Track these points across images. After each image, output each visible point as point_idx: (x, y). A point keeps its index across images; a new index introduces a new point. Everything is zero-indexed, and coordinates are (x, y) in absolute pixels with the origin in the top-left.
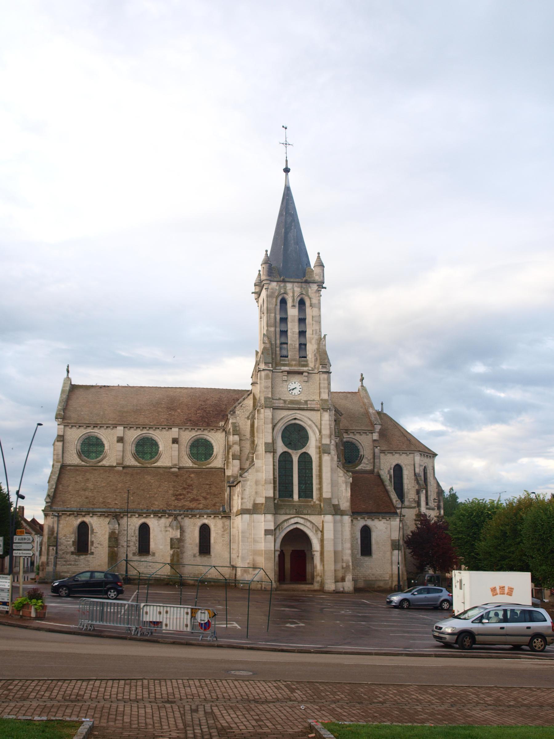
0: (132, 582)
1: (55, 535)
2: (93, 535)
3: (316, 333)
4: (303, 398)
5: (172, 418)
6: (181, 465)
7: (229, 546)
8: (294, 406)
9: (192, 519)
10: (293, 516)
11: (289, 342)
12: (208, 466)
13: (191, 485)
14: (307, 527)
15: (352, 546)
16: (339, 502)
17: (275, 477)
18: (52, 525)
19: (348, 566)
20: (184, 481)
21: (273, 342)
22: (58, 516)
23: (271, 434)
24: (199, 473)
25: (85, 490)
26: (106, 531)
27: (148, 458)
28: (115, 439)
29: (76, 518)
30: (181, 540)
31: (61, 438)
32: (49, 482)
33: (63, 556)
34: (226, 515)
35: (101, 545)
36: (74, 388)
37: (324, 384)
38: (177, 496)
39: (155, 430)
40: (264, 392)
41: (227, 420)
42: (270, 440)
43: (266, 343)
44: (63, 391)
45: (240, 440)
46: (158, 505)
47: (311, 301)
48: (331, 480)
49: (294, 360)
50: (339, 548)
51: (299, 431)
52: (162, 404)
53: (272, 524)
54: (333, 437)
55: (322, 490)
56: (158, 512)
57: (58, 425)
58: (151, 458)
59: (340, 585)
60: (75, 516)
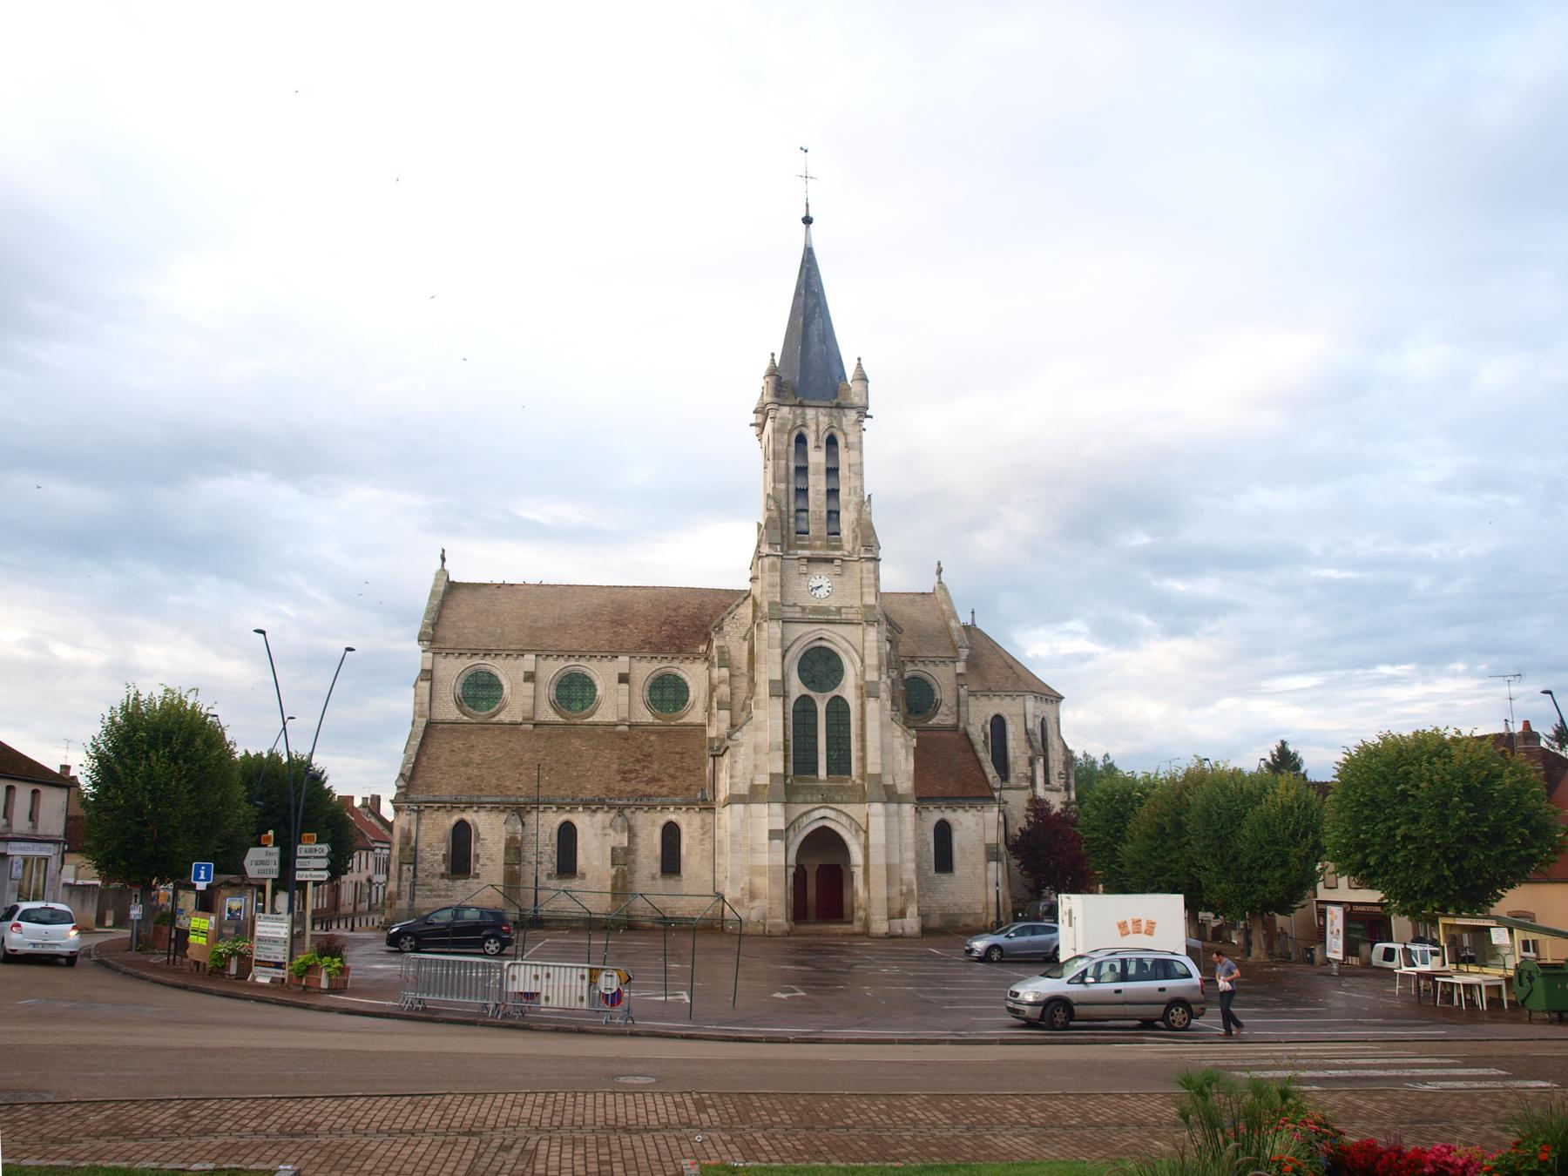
0: (546, 924)
1: (413, 844)
3: (855, 493)
4: (833, 603)
5: (619, 638)
6: (633, 720)
7: (712, 860)
8: (819, 617)
9: (649, 814)
10: (817, 806)
11: (811, 509)
12: (679, 721)
13: (650, 755)
14: (842, 824)
15: (918, 855)
16: (894, 780)
17: (787, 738)
18: (407, 828)
19: (910, 891)
20: (638, 748)
21: (784, 509)
22: (419, 812)
23: (780, 666)
24: (663, 733)
25: (467, 765)
26: (500, 837)
27: (578, 708)
28: (521, 676)
29: (450, 813)
30: (629, 851)
31: (428, 675)
32: (405, 752)
33: (426, 880)
34: (708, 806)
35: (492, 861)
36: (452, 588)
37: (869, 579)
38: (625, 773)
39: (589, 660)
40: (768, 593)
41: (710, 642)
42: (778, 676)
43: (772, 510)
44: (433, 594)
45: (731, 676)
46: (592, 789)
47: (846, 439)
48: (882, 744)
50: (896, 860)
51: (828, 659)
52: (602, 615)
53: (783, 819)
54: (884, 669)
55: (866, 761)
56: (591, 802)
57: (423, 651)
58: (583, 708)
59: (897, 923)
60: (448, 811)
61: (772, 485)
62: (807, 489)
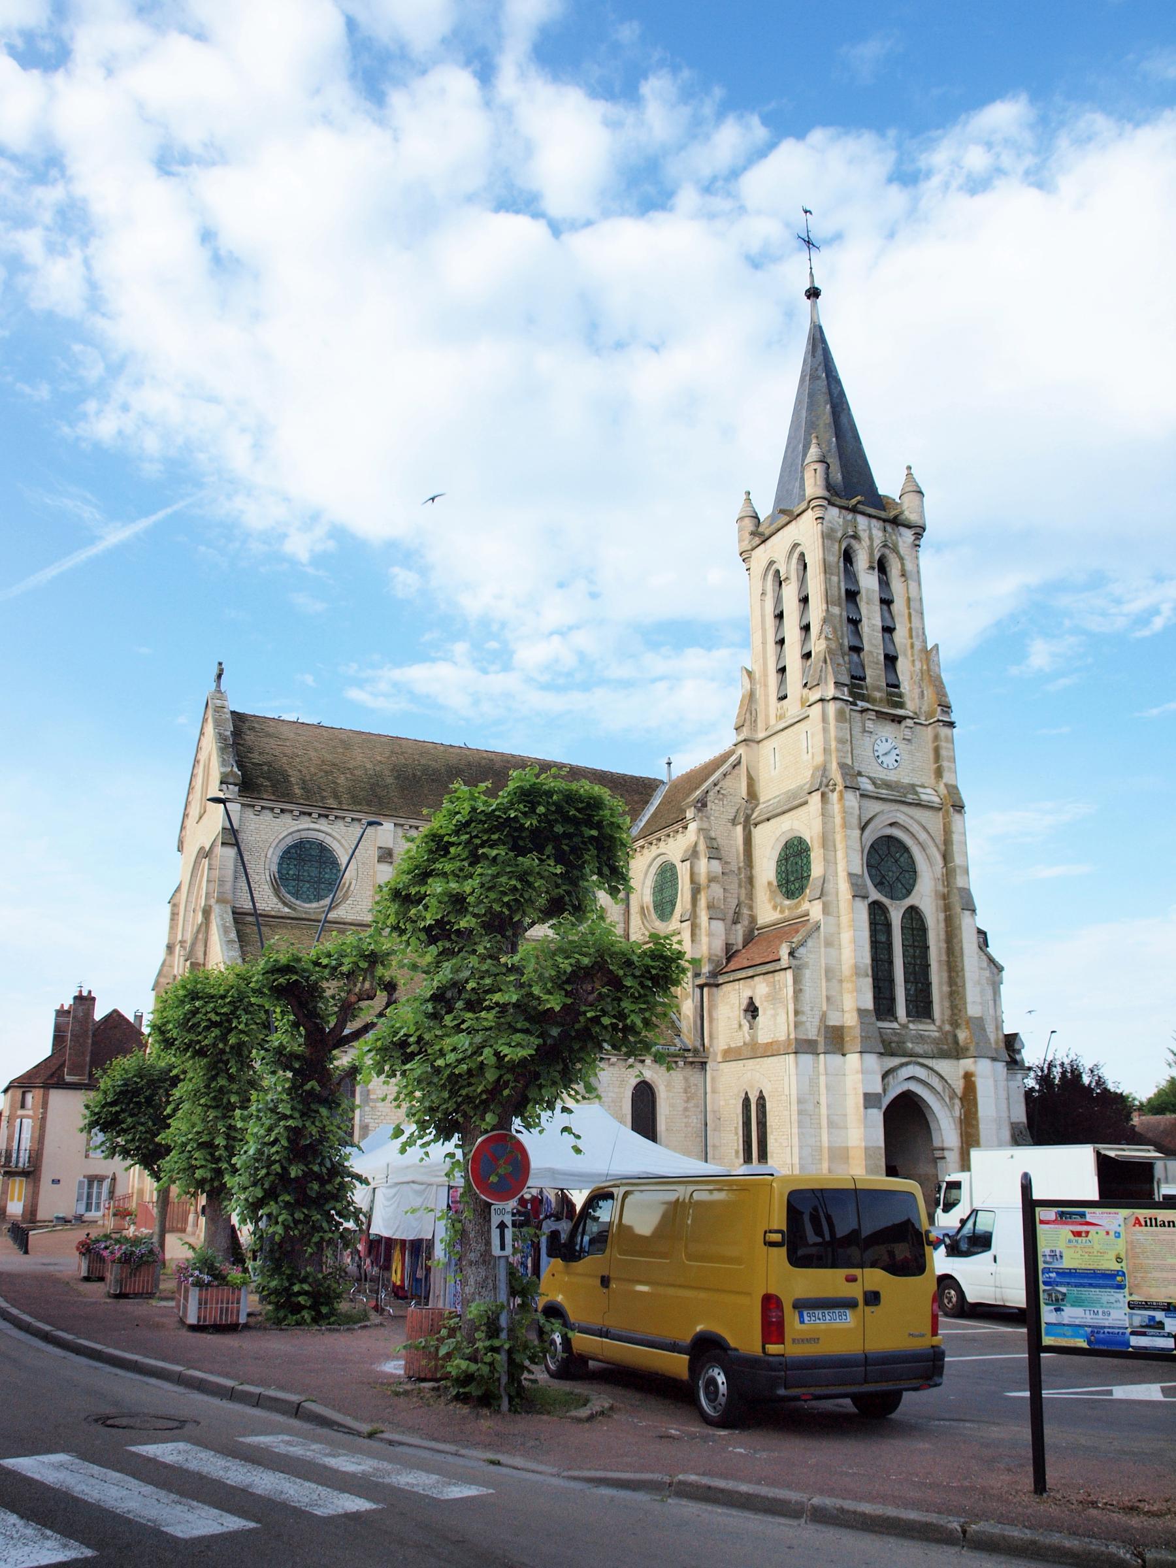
2: (367, 1109)
3: (918, 636)
9: (616, 1068)
11: (866, 647)
43: (830, 639)
49: (878, 689)
61: (824, 606)
62: (860, 620)
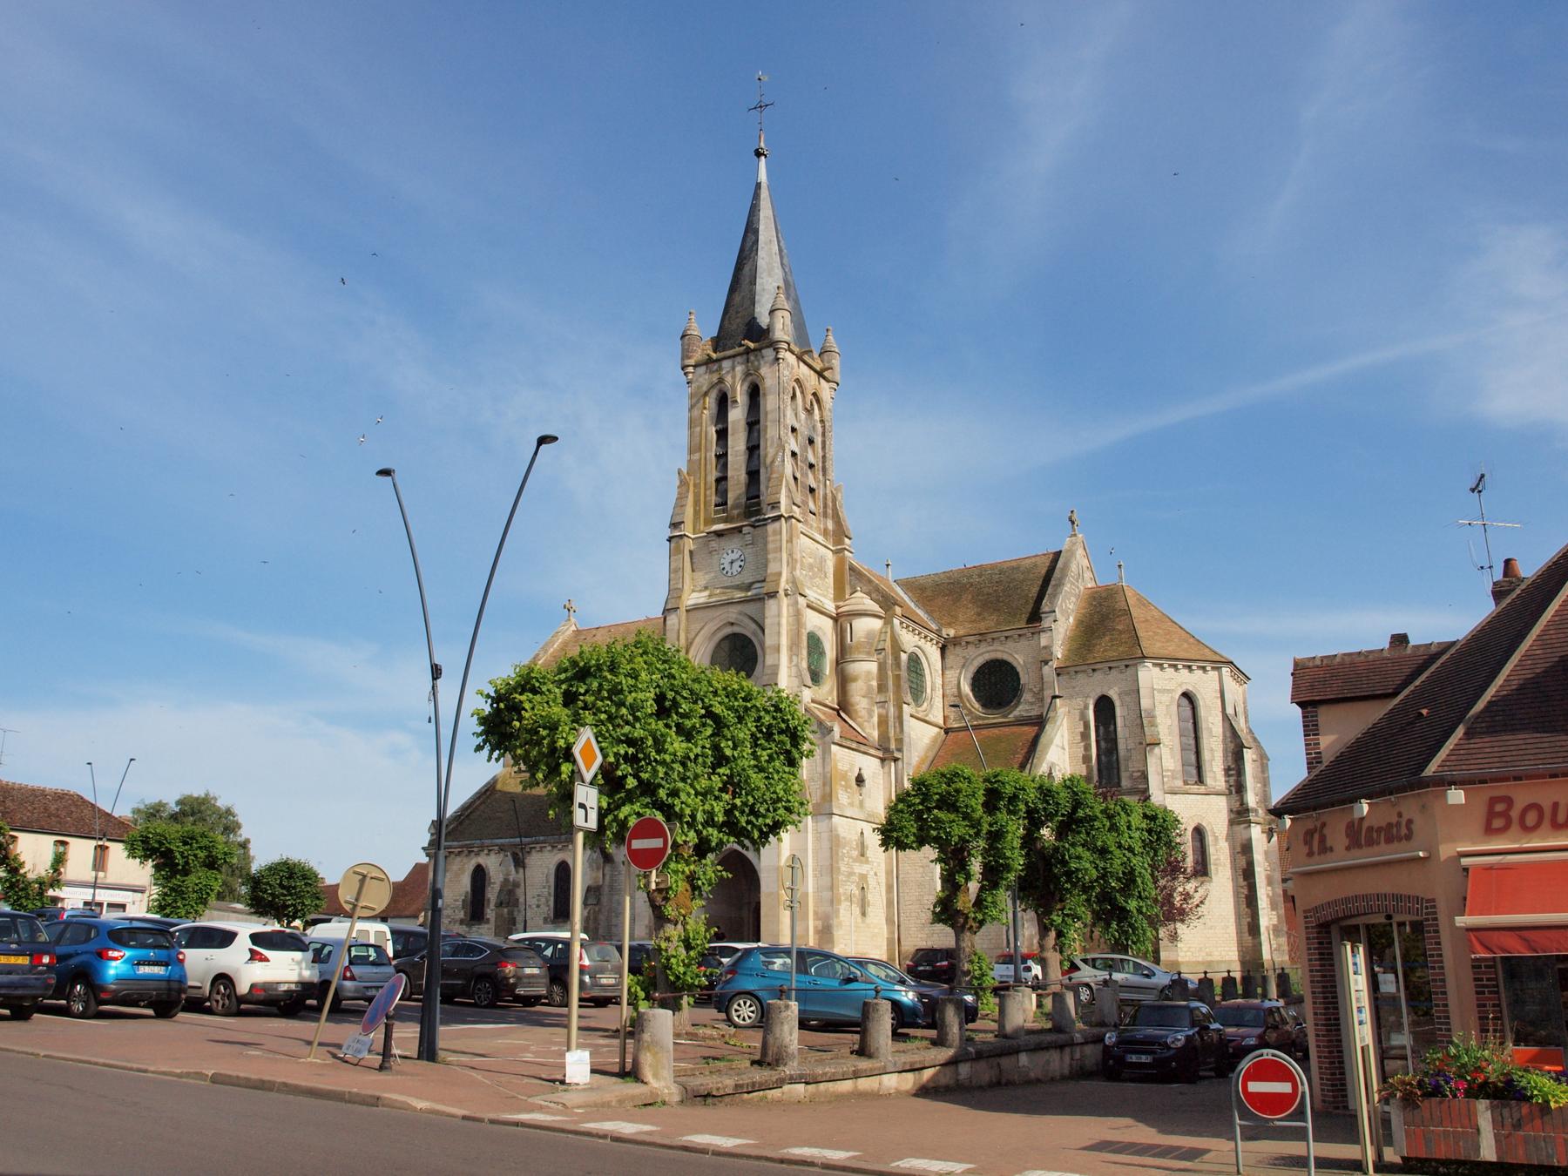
3: (773, 442)
11: (730, 474)
